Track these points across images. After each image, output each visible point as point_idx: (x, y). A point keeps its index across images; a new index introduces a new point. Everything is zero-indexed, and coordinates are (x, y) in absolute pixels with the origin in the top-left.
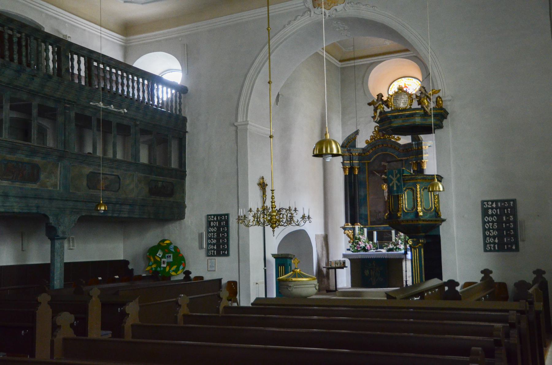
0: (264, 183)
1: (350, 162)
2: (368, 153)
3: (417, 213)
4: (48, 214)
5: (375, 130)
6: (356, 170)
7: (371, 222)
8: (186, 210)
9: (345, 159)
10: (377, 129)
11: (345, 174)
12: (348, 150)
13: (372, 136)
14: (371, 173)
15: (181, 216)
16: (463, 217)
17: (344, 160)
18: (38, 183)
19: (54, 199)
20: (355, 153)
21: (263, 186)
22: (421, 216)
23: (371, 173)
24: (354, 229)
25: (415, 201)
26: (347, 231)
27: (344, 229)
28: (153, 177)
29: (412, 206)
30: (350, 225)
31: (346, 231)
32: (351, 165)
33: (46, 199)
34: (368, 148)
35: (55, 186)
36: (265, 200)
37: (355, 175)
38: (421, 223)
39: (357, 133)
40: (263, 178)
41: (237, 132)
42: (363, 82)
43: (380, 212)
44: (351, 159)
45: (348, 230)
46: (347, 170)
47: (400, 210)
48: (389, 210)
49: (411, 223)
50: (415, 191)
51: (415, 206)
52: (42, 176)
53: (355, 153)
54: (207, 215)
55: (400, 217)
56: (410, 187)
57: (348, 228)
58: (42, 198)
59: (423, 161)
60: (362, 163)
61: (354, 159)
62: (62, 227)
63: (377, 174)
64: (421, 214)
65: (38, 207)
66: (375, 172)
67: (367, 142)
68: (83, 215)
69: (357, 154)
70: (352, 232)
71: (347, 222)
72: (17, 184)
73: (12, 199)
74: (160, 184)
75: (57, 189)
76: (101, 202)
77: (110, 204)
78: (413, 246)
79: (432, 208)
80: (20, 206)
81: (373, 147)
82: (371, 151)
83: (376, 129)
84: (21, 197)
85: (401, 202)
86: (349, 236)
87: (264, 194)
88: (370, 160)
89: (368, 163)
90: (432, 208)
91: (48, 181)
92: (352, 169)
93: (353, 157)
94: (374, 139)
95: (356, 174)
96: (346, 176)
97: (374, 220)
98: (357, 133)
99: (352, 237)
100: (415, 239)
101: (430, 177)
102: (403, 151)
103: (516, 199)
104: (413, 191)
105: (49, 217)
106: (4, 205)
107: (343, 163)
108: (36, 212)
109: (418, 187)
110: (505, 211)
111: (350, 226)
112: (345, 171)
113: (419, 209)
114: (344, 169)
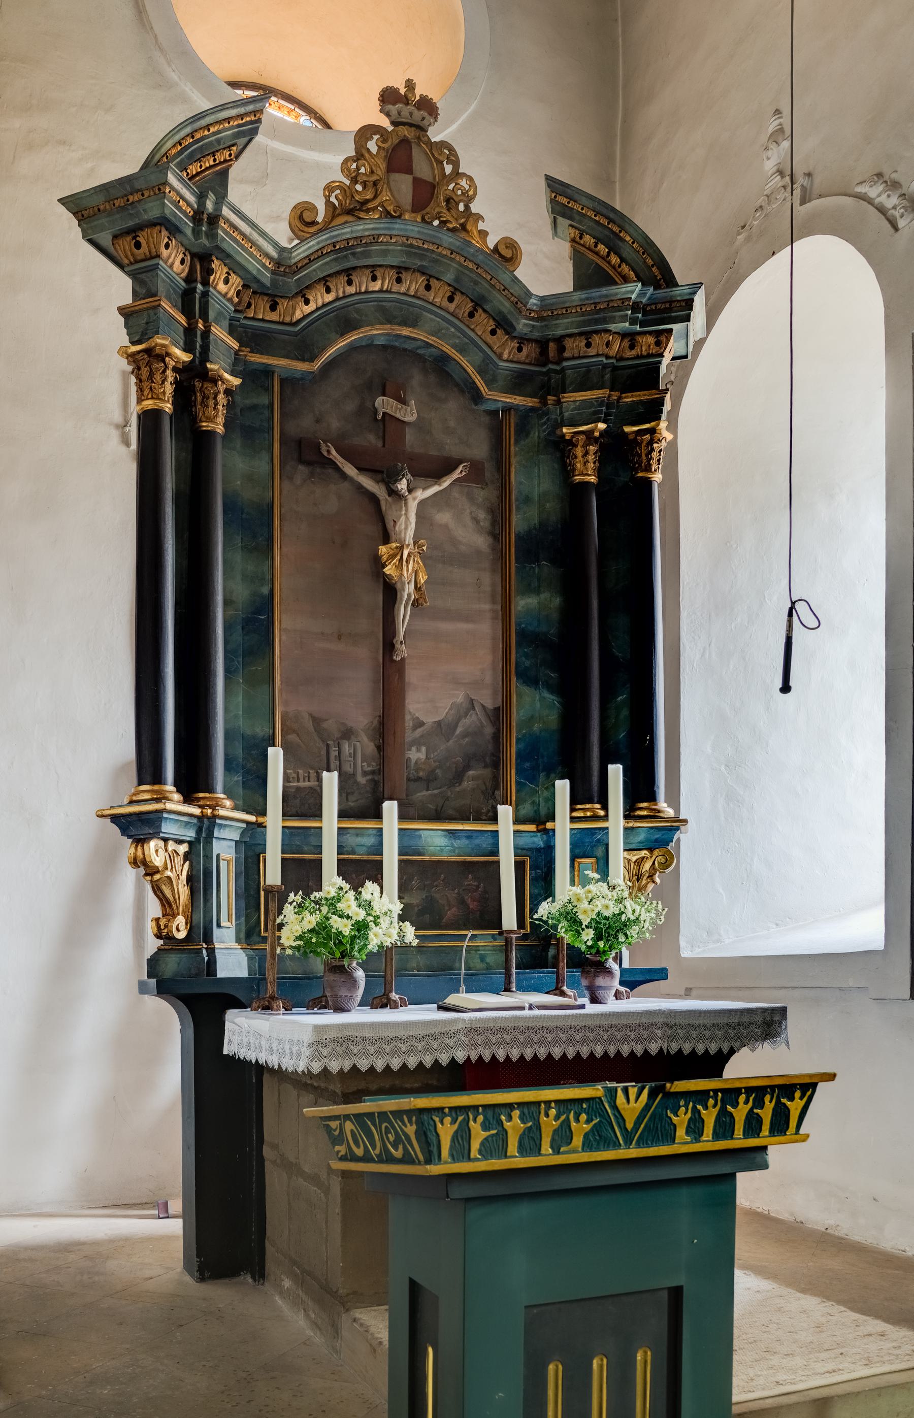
6: (221, 397)
10: (372, 146)
11: (149, 404)
13: (341, 187)
26: (155, 852)
30: (177, 797)
31: (153, 844)
34: (310, 260)
43: (347, 734)
45: (165, 840)
46: (170, 375)
61: (212, 315)
63: (350, 470)
66: (334, 452)
67: (308, 217)
70: (187, 856)
81: (338, 273)
82: (320, 298)
83: (372, 146)
88: (312, 359)
93: (205, 294)
95: (211, 434)
97: (307, 784)
102: (520, 350)
112: (158, 377)
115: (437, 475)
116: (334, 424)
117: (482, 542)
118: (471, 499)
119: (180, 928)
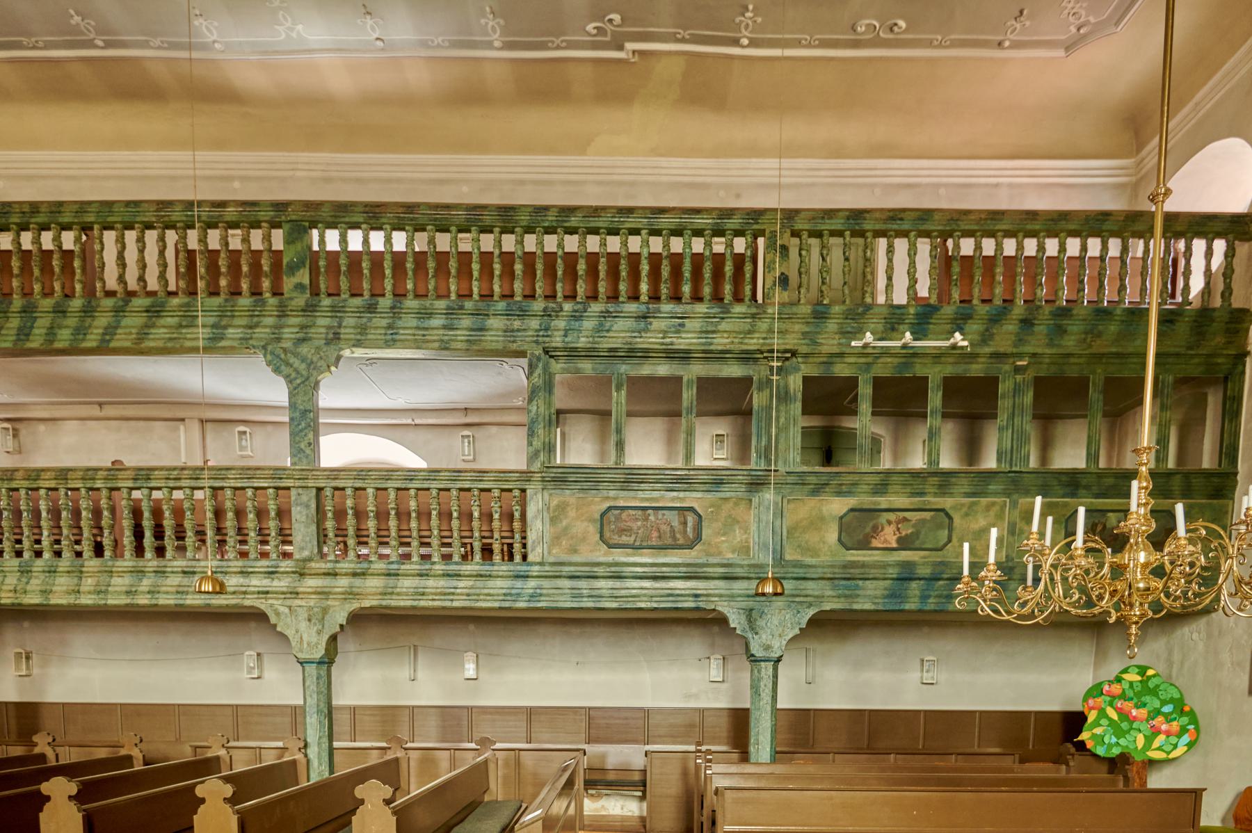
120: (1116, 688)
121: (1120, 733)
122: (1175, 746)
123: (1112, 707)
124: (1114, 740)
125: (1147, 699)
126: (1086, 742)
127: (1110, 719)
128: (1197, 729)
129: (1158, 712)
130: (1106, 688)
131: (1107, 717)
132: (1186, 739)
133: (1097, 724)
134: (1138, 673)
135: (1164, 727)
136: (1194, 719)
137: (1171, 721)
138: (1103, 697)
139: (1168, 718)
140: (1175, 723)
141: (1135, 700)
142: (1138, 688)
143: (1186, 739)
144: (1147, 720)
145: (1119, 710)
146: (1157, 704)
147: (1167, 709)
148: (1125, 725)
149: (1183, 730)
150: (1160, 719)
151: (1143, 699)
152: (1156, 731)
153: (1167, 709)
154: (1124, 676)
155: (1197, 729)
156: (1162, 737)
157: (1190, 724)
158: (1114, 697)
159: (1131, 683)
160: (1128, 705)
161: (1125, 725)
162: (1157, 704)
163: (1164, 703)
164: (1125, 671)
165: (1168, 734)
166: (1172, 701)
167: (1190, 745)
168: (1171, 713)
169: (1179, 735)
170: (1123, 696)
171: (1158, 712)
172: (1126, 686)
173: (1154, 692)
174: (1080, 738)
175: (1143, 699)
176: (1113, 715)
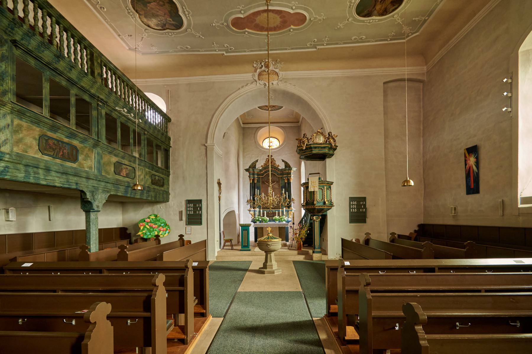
0: (220, 182)
1: (253, 175)
2: (262, 172)
3: (324, 203)
4: (85, 190)
5: (266, 160)
7: (262, 208)
8: (170, 196)
9: (251, 174)
10: (267, 160)
12: (253, 170)
13: (265, 163)
14: (263, 182)
15: (167, 200)
16: (339, 205)
17: (250, 175)
18: (77, 163)
19: (90, 179)
20: (256, 172)
21: (219, 184)
22: (327, 204)
23: (263, 182)
24: (255, 211)
25: (323, 196)
27: (250, 211)
28: (154, 172)
29: (321, 198)
32: (253, 178)
33: (84, 178)
35: (90, 168)
36: (221, 192)
37: (255, 183)
38: (325, 207)
39: (257, 161)
40: (219, 180)
41: (206, 149)
42: (254, 137)
44: (253, 174)
47: (315, 200)
48: (306, 200)
49: (321, 207)
50: (323, 190)
51: (323, 198)
52: (81, 158)
53: (256, 172)
54: (186, 199)
55: (316, 204)
56: (321, 188)
57: (252, 210)
58: (81, 177)
59: (291, 178)
60: (259, 177)
62: (97, 202)
64: (327, 203)
65: (77, 184)
68: (112, 194)
69: (257, 172)
71: (251, 207)
72: (58, 161)
73: (53, 174)
74: (157, 178)
75: (92, 170)
76: (138, 183)
77: (130, 188)
78: (315, 220)
79: (329, 200)
80: (61, 181)
82: (264, 171)
84: (63, 173)
85: (316, 196)
86: (252, 215)
87: (220, 189)
89: (262, 177)
90: (329, 200)
91: (85, 163)
92: (253, 180)
94: (266, 165)
96: (250, 183)
98: (257, 161)
99: (253, 215)
100: (317, 217)
101: (330, 183)
103: (366, 197)
104: (322, 190)
105: (86, 193)
106: (46, 178)
107: (249, 177)
108: (75, 188)
109: (325, 188)
110: (360, 203)
111: (252, 209)
113: (326, 200)
114: (250, 179)
115: (274, 182)
116: (266, 180)
117: (278, 187)
118: (277, 184)
119: (253, 217)
120: (148, 220)
121: (150, 232)
122: (165, 233)
123: (147, 225)
124: (149, 234)
125: (157, 222)
126: (141, 235)
127: (148, 228)
128: (170, 229)
129: (160, 226)
130: (146, 220)
131: (146, 228)
132: (167, 232)
133: (143, 229)
134: (154, 216)
135: (162, 229)
136: (169, 227)
137: (164, 227)
138: (145, 222)
139: (163, 227)
140: (165, 228)
141: (154, 223)
142: (154, 220)
143: (167, 232)
144: (158, 228)
145: (150, 226)
146: (160, 224)
147: (162, 225)
148: (152, 230)
149: (167, 230)
150: (161, 227)
151: (156, 223)
152: (160, 230)
153: (162, 225)
154: (150, 217)
155: (170, 229)
156: (162, 232)
157: (168, 228)
158: (148, 222)
159: (152, 219)
160: (152, 224)
161: (152, 230)
162: (160, 224)
163: (161, 223)
164: (151, 215)
165: (163, 231)
166: (163, 223)
167: (169, 233)
168: (164, 226)
169: (166, 231)
170: (151, 222)
171: (160, 226)
172: (151, 219)
173: (159, 221)
174: (138, 234)
175: (156, 223)
176: (149, 227)
